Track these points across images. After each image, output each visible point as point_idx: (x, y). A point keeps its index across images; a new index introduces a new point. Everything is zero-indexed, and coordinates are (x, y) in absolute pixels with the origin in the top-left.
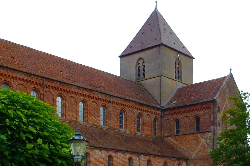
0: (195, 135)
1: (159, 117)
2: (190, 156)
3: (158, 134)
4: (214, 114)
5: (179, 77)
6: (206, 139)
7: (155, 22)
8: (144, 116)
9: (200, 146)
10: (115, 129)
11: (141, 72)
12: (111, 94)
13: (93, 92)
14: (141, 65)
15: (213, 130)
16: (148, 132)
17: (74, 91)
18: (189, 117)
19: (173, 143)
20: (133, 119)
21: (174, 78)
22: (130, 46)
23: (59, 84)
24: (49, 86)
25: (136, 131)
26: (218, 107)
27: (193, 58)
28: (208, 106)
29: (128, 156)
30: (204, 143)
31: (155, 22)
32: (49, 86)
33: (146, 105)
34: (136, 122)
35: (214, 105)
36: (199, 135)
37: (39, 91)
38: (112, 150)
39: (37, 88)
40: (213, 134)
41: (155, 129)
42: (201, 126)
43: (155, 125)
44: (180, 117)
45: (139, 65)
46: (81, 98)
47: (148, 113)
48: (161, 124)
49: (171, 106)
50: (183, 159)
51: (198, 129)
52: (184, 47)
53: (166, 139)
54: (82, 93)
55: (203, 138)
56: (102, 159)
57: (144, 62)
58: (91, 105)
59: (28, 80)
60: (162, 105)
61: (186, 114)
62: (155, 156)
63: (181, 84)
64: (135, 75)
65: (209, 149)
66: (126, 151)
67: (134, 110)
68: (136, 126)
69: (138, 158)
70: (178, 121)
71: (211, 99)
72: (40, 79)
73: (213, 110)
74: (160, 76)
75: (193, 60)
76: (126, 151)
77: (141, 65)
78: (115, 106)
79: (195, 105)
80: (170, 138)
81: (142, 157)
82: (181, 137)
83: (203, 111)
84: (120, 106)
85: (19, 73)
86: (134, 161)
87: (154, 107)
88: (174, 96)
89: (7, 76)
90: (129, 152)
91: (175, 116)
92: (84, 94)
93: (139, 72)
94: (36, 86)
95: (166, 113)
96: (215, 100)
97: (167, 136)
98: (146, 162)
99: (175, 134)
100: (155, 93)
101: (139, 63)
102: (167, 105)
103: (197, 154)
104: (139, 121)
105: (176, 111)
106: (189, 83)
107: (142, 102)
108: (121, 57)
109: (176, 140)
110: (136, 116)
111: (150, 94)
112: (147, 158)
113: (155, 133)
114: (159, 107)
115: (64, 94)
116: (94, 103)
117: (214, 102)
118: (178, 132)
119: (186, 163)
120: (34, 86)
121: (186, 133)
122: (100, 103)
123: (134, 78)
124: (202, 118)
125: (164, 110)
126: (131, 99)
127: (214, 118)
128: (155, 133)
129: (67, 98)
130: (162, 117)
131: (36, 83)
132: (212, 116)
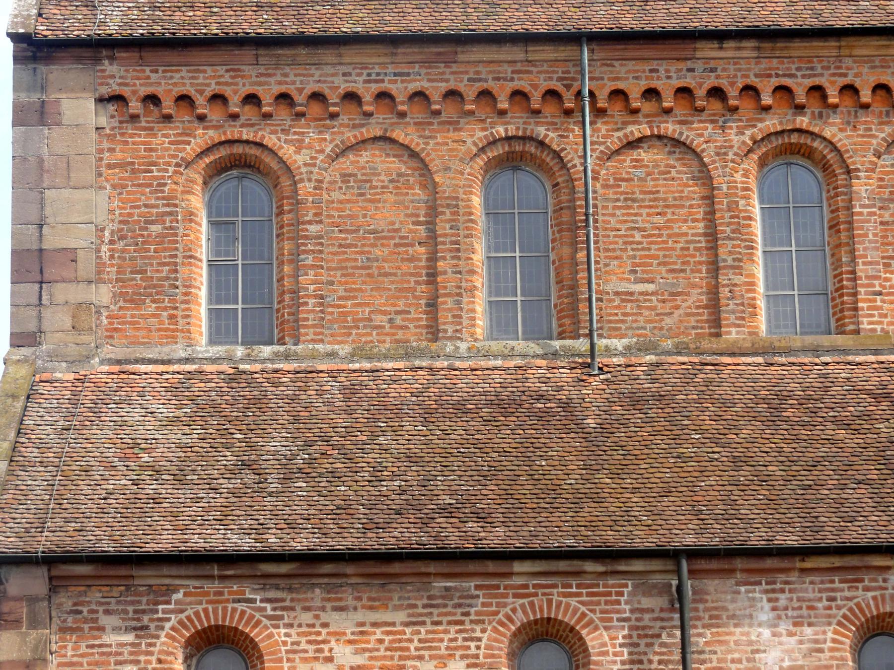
23: (754, 54)
24: (651, 93)
32: (651, 93)
37: (557, 155)
39: (531, 139)
59: (436, 90)
72: (552, 56)
85: (340, 55)
89: (168, 106)
120: (500, 131)
131: (519, 95)
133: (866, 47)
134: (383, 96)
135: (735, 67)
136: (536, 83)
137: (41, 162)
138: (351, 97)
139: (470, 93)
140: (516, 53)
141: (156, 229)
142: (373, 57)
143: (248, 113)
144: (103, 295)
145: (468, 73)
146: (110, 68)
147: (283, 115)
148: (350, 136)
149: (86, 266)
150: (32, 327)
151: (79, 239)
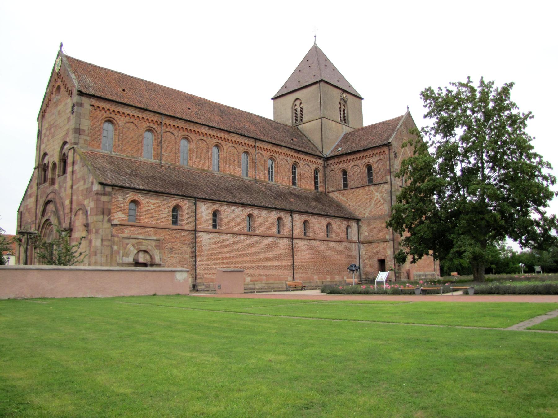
0: (368, 188)
1: (321, 168)
2: (362, 216)
3: (321, 189)
4: (390, 161)
5: (345, 120)
6: (381, 193)
7: (315, 56)
8: (301, 166)
9: (374, 202)
10: (261, 181)
11: (298, 116)
12: (256, 137)
13: (232, 134)
14: (298, 107)
15: (389, 180)
16: (306, 185)
17: (205, 132)
18: (358, 166)
19: (340, 199)
20: (287, 170)
21: (339, 121)
22: (285, 86)
24: (170, 125)
25: (291, 184)
26: (395, 152)
27: (361, 98)
28: (382, 151)
29: (276, 215)
30: (379, 198)
31: (315, 56)
32: (170, 125)
33: (303, 152)
34: (291, 174)
35: (389, 149)
36: (372, 188)
38: (253, 206)
40: (390, 186)
41: (316, 183)
42: (374, 175)
43: (316, 178)
44: (347, 166)
45: (296, 108)
46: (215, 141)
47: (307, 163)
48: (325, 177)
49: (336, 154)
50: (353, 219)
51: (370, 181)
52: (350, 86)
53: (331, 195)
54: (216, 135)
55: (377, 191)
56: (239, 219)
57: (301, 103)
58: (229, 150)
60: (324, 153)
61: (355, 163)
62: (314, 214)
63: (348, 128)
64: (291, 119)
65: (386, 205)
66: (274, 208)
67: (287, 159)
68: (291, 179)
69: (290, 218)
70: (345, 173)
71: (385, 142)
73: (388, 156)
74: (321, 118)
75: (363, 101)
76: (274, 208)
77: (298, 107)
78: (263, 152)
79: (365, 150)
80: (335, 193)
81: (296, 217)
82: (350, 191)
83: (376, 158)
84: (269, 152)
86: (284, 219)
87: (315, 155)
88: (340, 142)
90: (276, 209)
91: (341, 166)
92: (219, 136)
93: (296, 115)
94: (151, 125)
95: (330, 162)
96: (390, 143)
97: (332, 192)
98: (302, 223)
99: (342, 188)
100: (316, 139)
101: (296, 105)
102: (331, 152)
103: (369, 213)
104: (295, 172)
105: (342, 159)
106: (357, 127)
107: (297, 148)
108: (274, 99)
109: (343, 196)
110: (291, 166)
111: (309, 141)
112: (303, 217)
113: (317, 188)
114: (321, 155)
115: (192, 136)
116: (233, 148)
117: (388, 145)
118: (345, 185)
119: (358, 224)
121: (356, 186)
122: (242, 148)
123: (289, 123)
124: (374, 167)
125: (326, 159)
126: (283, 144)
127: (390, 165)
128: (317, 188)
129: (195, 141)
130: (325, 167)
132: (388, 163)
133: (197, 125)
134: (133, 116)
135: (181, 124)
136: (155, 119)
137: (80, 114)
138: (128, 115)
139: (146, 118)
140: (152, 114)
141: (97, 129)
142: (132, 109)
143: (113, 113)
144: (88, 138)
145: (146, 115)
146: (92, 100)
147: (118, 115)
148: (128, 121)
149: (86, 133)
150: (77, 141)
151: (86, 128)
